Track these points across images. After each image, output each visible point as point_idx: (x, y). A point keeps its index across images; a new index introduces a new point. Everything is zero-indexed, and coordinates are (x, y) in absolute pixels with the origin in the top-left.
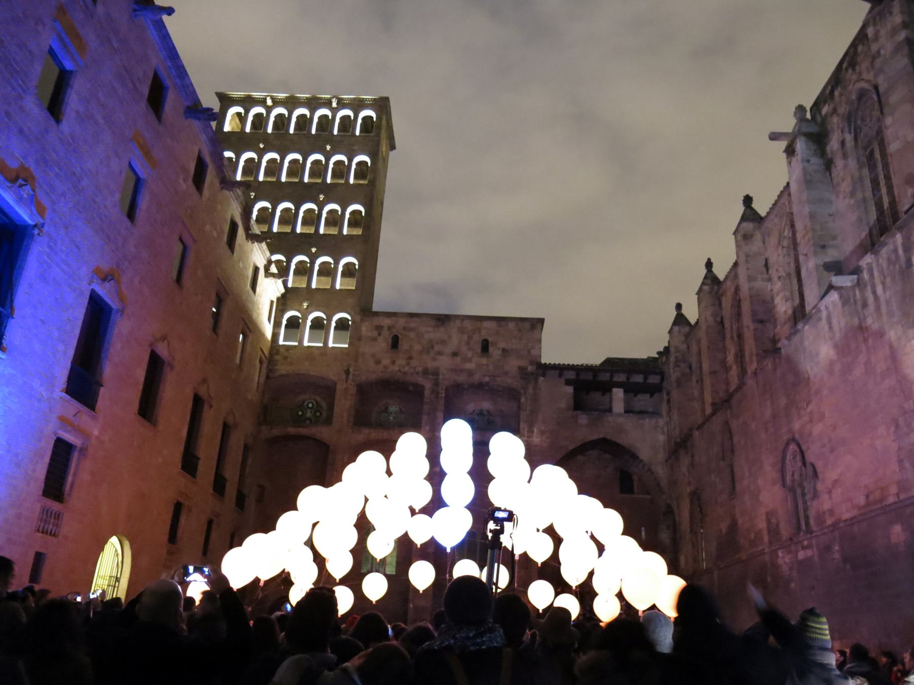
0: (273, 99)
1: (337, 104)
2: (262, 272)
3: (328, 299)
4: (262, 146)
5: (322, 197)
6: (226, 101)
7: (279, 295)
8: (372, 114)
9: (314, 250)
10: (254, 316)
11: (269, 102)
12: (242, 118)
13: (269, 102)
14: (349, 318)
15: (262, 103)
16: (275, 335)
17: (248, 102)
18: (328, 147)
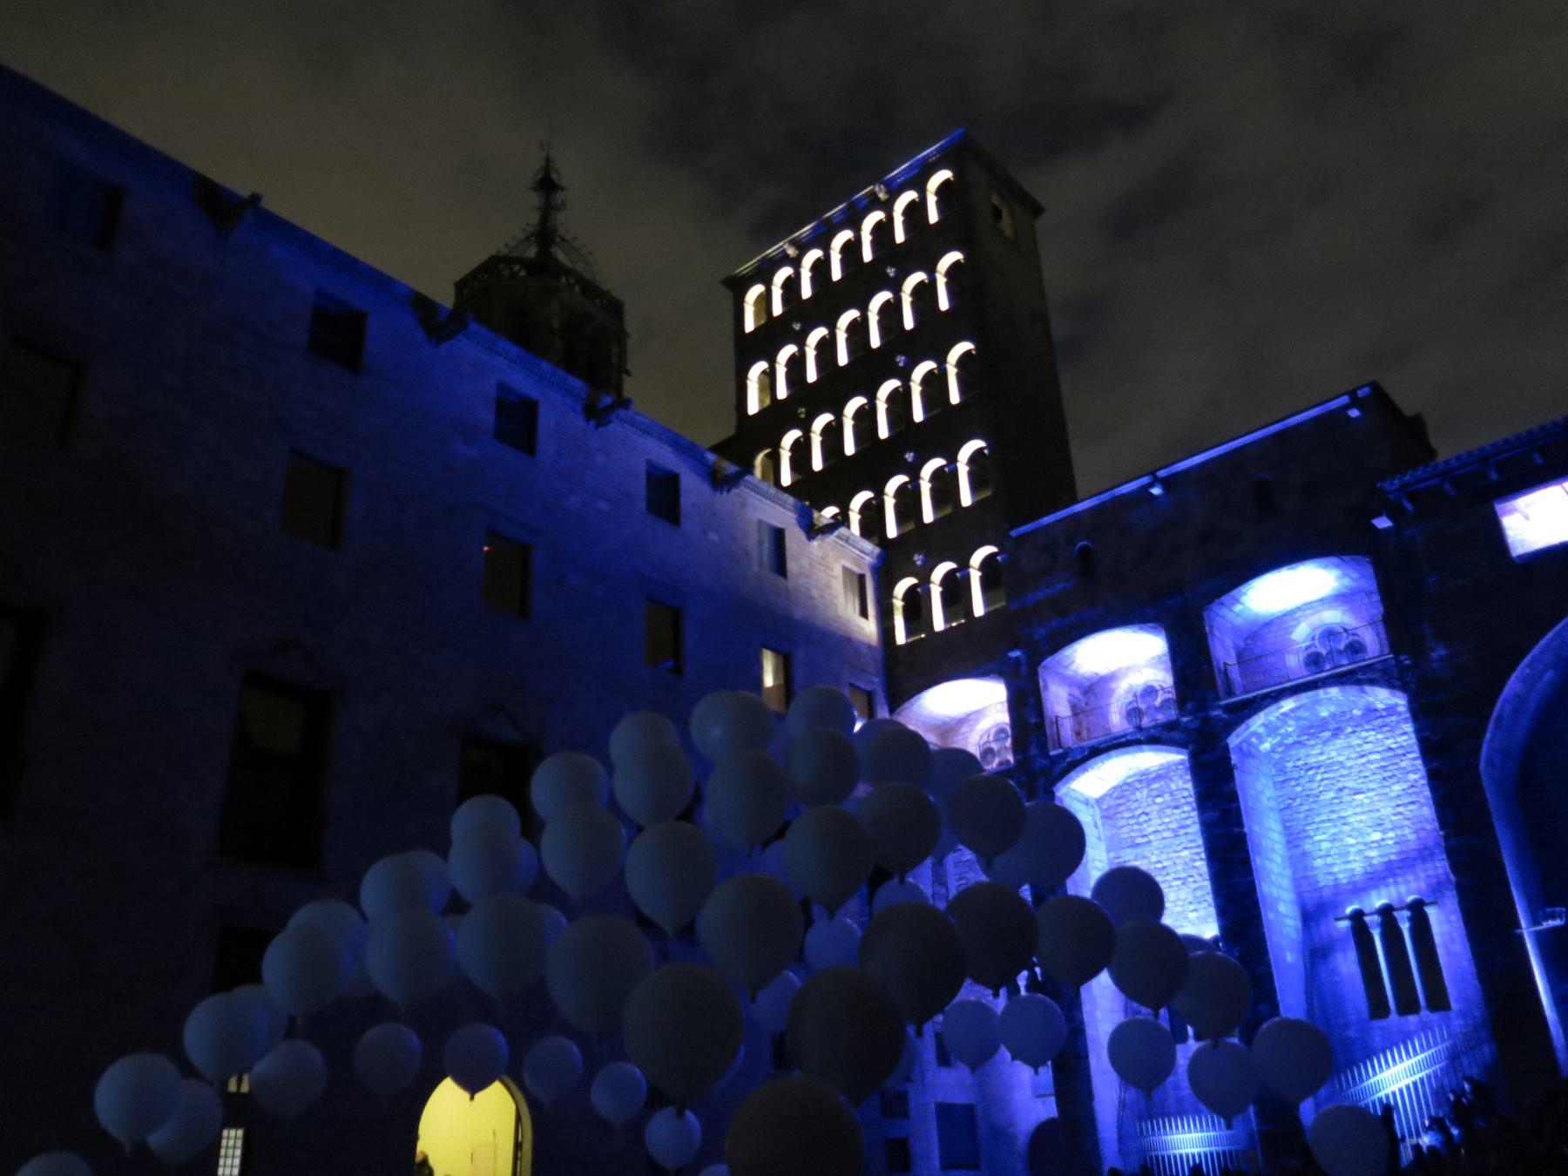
0: (793, 243)
1: (888, 192)
2: (795, 537)
3: (953, 535)
4: (797, 327)
5: (901, 360)
6: (738, 287)
7: (868, 559)
8: (944, 175)
9: (909, 456)
10: (798, 614)
11: (791, 252)
12: (766, 298)
13: (791, 252)
14: (989, 549)
15: (784, 260)
16: (887, 630)
17: (764, 274)
18: (891, 272)
